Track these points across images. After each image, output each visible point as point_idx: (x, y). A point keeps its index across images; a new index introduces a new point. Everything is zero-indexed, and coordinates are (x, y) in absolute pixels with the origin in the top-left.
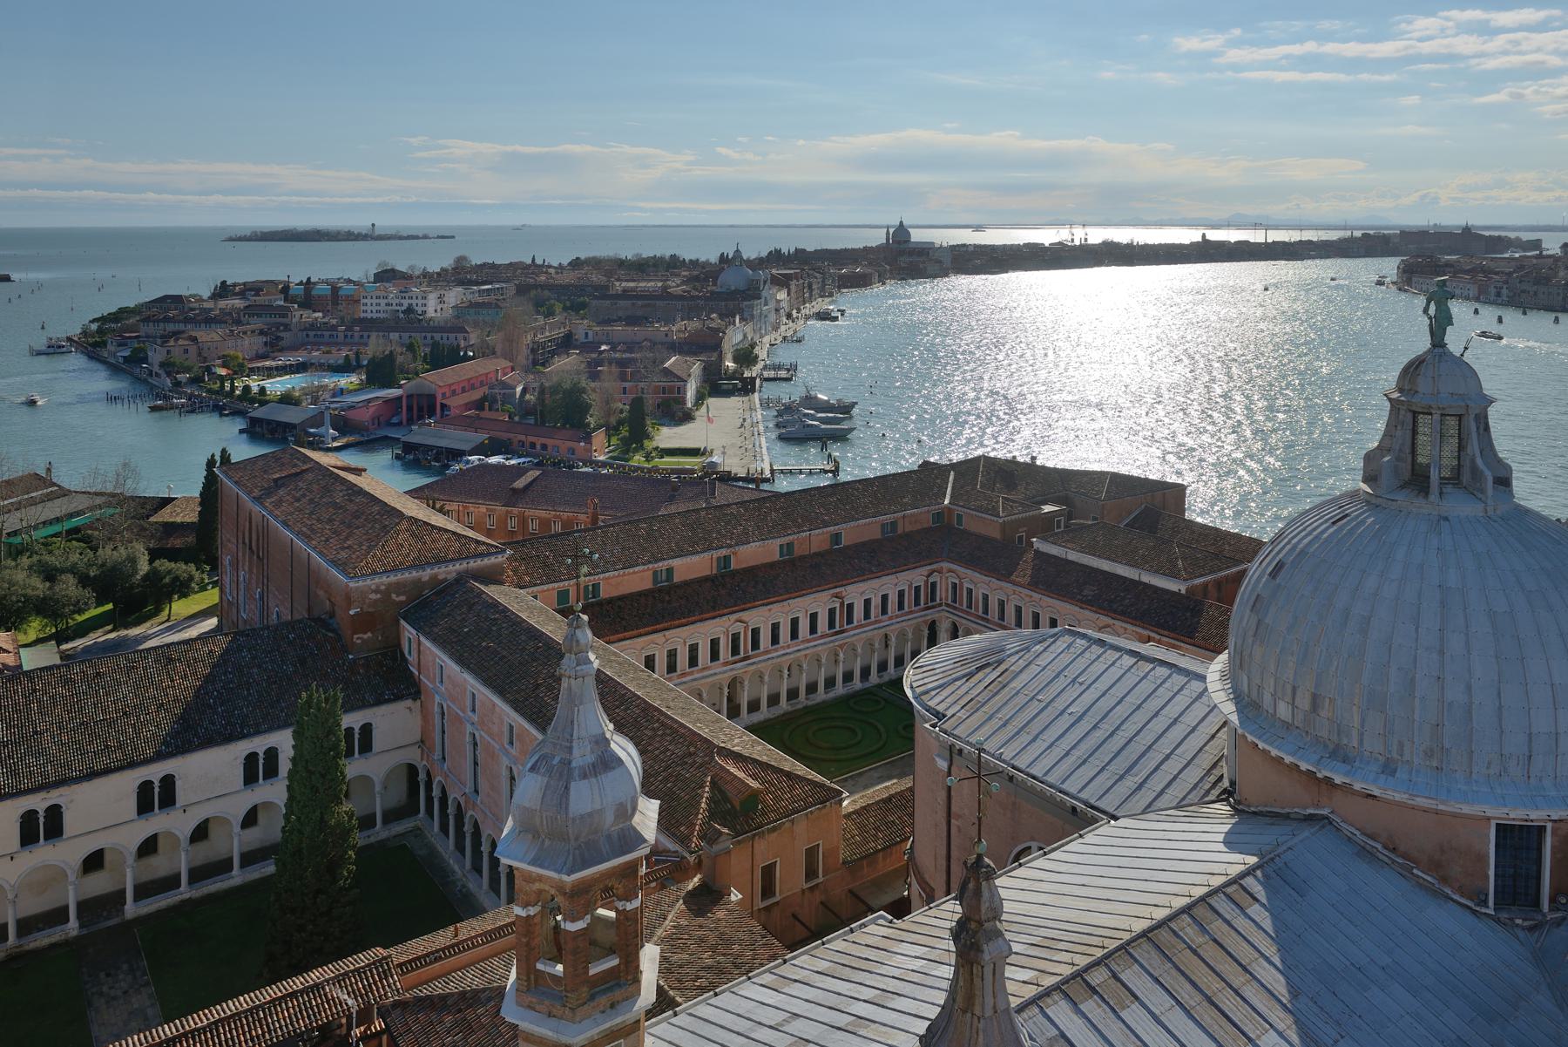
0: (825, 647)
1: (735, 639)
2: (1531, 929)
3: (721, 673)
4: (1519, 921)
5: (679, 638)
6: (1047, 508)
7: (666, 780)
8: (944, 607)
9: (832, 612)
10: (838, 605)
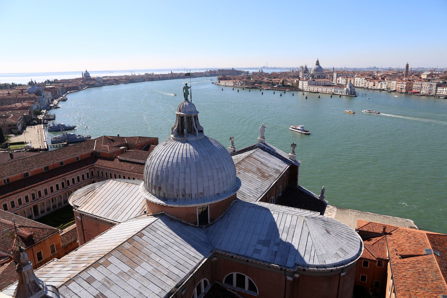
0: (62, 193)
1: (33, 195)
2: (206, 227)
3: (30, 205)
4: (204, 226)
5: (14, 198)
6: (122, 148)
7: (3, 238)
8: (96, 177)
9: (63, 183)
10: (64, 181)
